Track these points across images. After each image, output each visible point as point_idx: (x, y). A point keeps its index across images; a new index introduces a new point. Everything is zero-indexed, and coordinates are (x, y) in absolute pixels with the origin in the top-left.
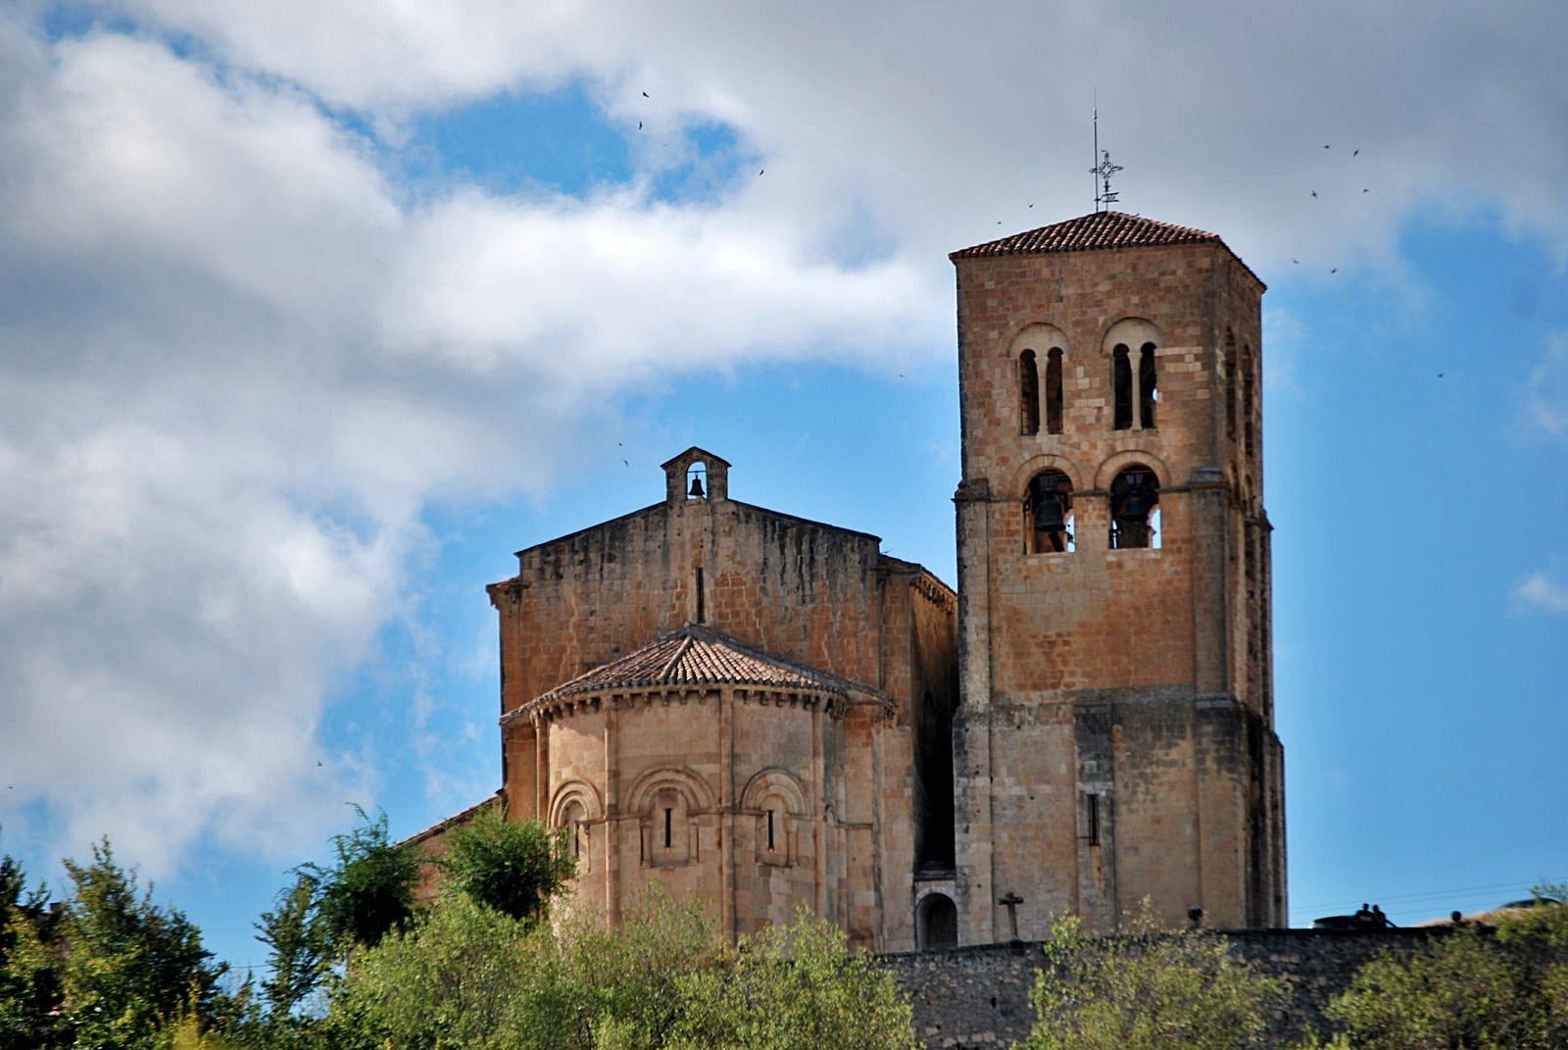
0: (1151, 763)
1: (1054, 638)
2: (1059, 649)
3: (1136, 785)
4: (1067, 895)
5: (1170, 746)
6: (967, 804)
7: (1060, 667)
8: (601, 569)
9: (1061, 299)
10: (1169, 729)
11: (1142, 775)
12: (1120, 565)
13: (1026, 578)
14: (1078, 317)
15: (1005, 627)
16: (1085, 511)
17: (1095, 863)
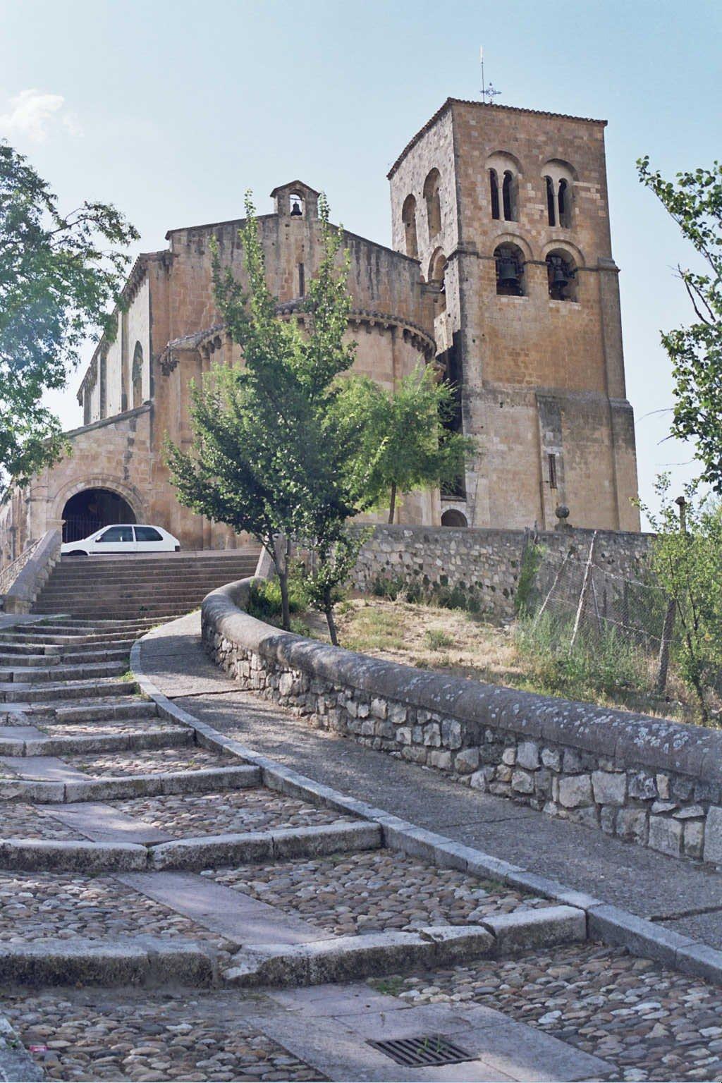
2: (521, 358)
5: (594, 429)
7: (523, 370)
8: (232, 252)
10: (594, 418)
12: (558, 311)
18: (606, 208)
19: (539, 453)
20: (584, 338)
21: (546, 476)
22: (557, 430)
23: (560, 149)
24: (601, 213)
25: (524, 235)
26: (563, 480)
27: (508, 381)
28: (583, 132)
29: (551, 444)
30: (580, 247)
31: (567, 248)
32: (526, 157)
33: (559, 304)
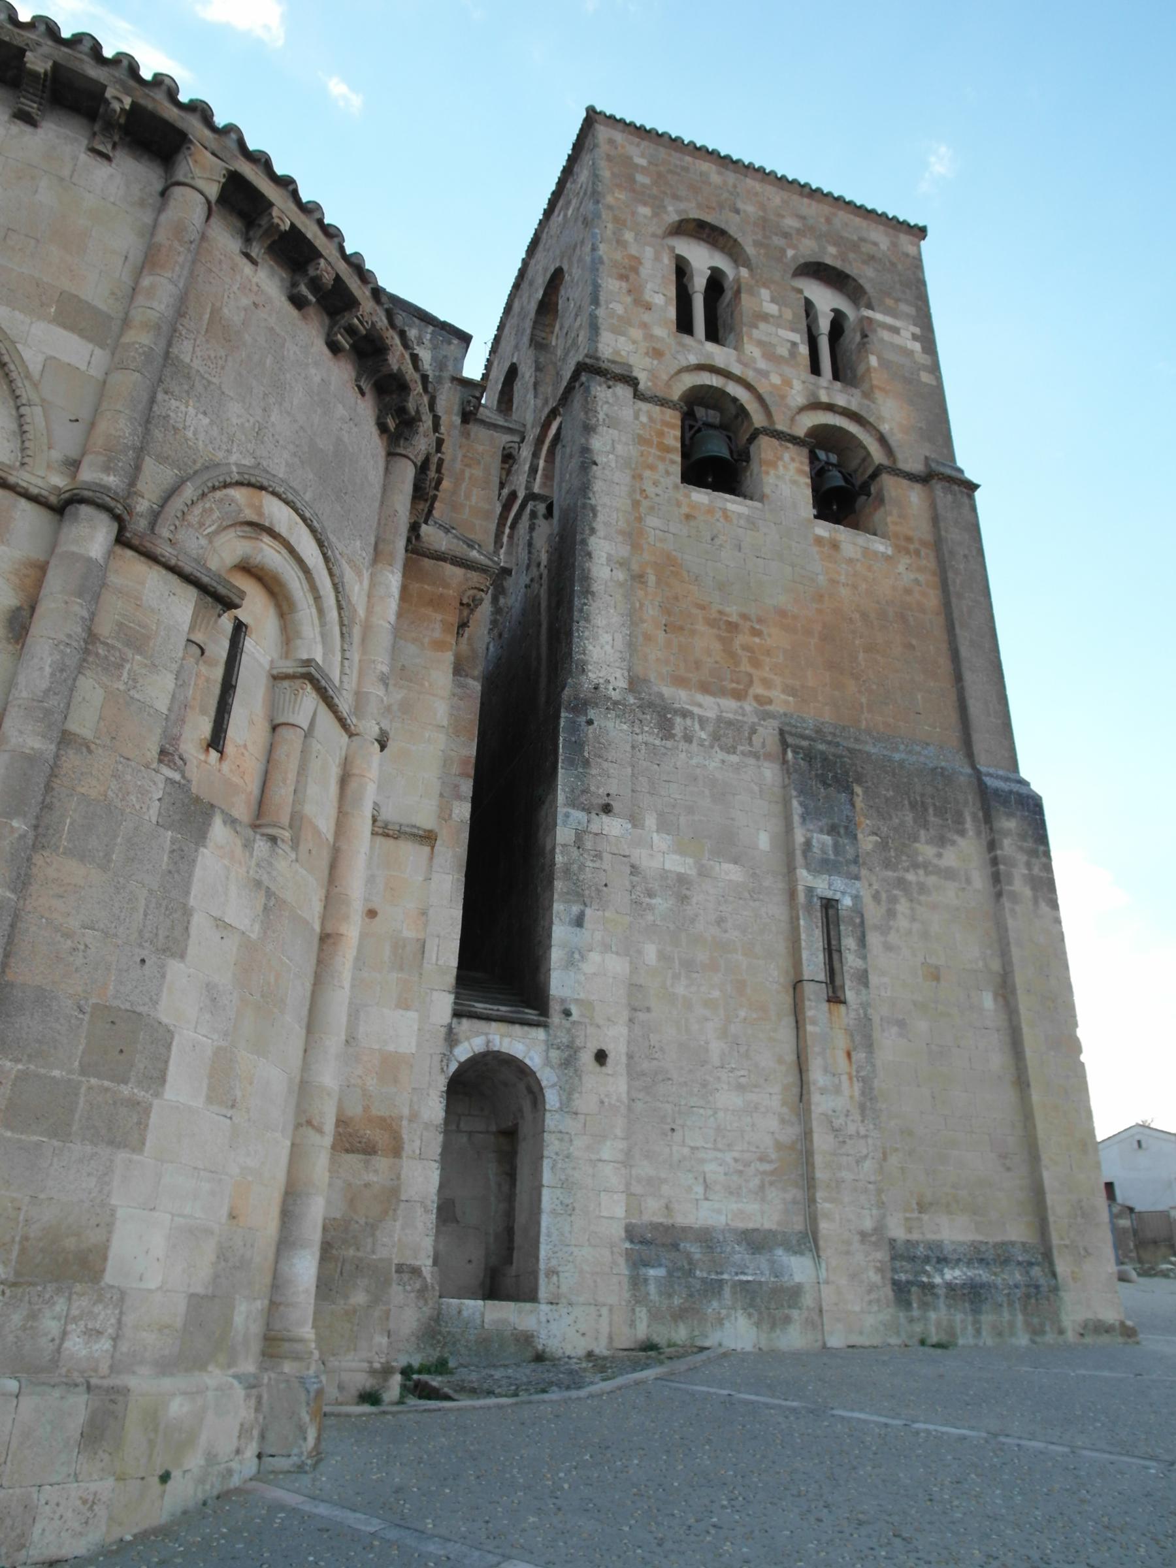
0: (915, 866)
1: (734, 618)
3: (893, 900)
4: (775, 1103)
5: (941, 841)
6: (582, 867)
7: (745, 666)
9: (737, 211)
10: (940, 812)
12: (835, 546)
13: (688, 517)
14: (759, 237)
15: (652, 579)
16: (781, 458)
18: (935, 369)
19: (792, 894)
21: (814, 965)
22: (844, 830)
23: (832, 250)
24: (925, 377)
25: (750, 376)
26: (863, 978)
27: (705, 688)
28: (880, 238)
29: (826, 866)
30: (885, 428)
32: (756, 244)
33: (842, 533)
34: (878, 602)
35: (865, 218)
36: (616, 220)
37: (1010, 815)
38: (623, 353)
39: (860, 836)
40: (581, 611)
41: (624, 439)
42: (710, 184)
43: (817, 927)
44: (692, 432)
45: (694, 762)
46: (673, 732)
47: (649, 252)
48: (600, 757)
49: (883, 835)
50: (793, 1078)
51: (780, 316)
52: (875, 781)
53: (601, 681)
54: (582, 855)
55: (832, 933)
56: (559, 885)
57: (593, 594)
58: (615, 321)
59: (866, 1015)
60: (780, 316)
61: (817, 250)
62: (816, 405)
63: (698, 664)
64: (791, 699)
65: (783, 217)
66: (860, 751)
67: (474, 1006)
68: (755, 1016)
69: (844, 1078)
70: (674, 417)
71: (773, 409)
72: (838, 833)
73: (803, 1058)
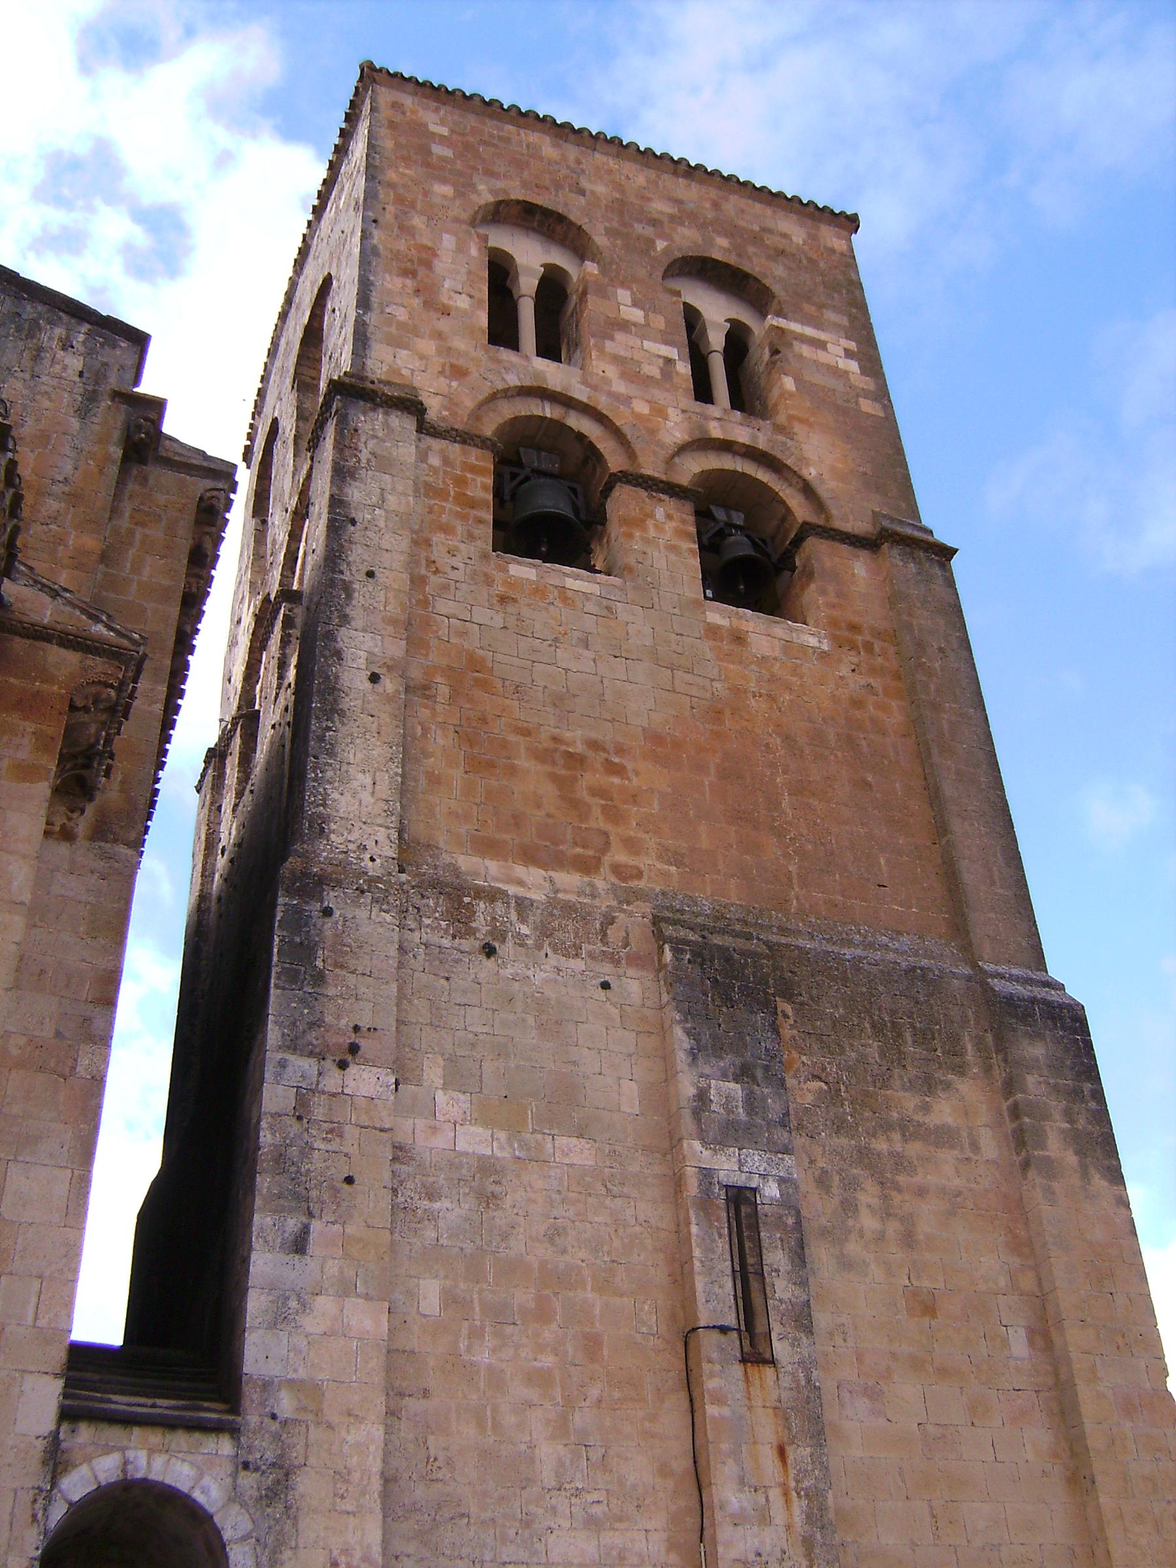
0: (887, 1127)
1: (579, 748)
2: (590, 778)
3: (851, 1185)
5: (928, 1085)
7: (597, 821)
10: (924, 1037)
11: (864, 1156)
12: (739, 638)
13: (503, 599)
14: (615, 224)
15: (443, 690)
16: (651, 515)
17: (768, 1431)
18: (882, 394)
19: (677, 1183)
20: (850, 742)
23: (722, 242)
24: (867, 406)
25: (603, 403)
26: (802, 1319)
27: (529, 856)
28: (795, 232)
30: (811, 473)
31: (763, 475)
32: (610, 232)
33: (751, 621)
34: (810, 720)
35: (769, 204)
36: (399, 200)
37: (1036, 1036)
38: (404, 372)
39: (791, 1082)
40: (322, 739)
41: (400, 488)
42: (541, 158)
43: (720, 1235)
44: (515, 483)
45: (508, 972)
46: (473, 925)
47: (448, 241)
48: (342, 967)
49: (831, 1079)
50: (688, 1501)
51: (647, 325)
52: (814, 992)
53: (352, 847)
54: (307, 1130)
55: (748, 1245)
56: (264, 1183)
57: (342, 714)
58: (393, 330)
59: (809, 1381)
60: (647, 325)
61: (700, 241)
62: (704, 444)
63: (517, 821)
64: (673, 869)
65: (649, 199)
66: (788, 946)
67: (110, 1401)
68: (616, 1395)
69: (775, 1494)
70: (483, 460)
71: (637, 446)
72: (754, 1078)
73: (702, 1462)
